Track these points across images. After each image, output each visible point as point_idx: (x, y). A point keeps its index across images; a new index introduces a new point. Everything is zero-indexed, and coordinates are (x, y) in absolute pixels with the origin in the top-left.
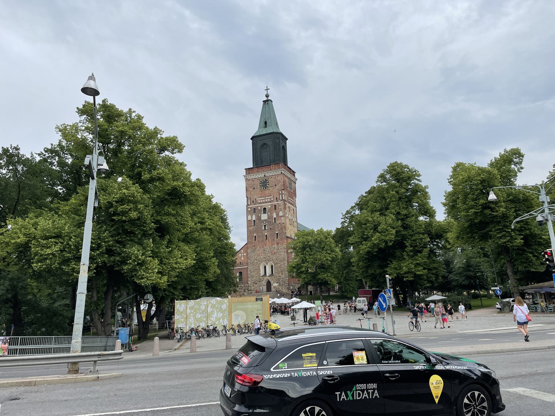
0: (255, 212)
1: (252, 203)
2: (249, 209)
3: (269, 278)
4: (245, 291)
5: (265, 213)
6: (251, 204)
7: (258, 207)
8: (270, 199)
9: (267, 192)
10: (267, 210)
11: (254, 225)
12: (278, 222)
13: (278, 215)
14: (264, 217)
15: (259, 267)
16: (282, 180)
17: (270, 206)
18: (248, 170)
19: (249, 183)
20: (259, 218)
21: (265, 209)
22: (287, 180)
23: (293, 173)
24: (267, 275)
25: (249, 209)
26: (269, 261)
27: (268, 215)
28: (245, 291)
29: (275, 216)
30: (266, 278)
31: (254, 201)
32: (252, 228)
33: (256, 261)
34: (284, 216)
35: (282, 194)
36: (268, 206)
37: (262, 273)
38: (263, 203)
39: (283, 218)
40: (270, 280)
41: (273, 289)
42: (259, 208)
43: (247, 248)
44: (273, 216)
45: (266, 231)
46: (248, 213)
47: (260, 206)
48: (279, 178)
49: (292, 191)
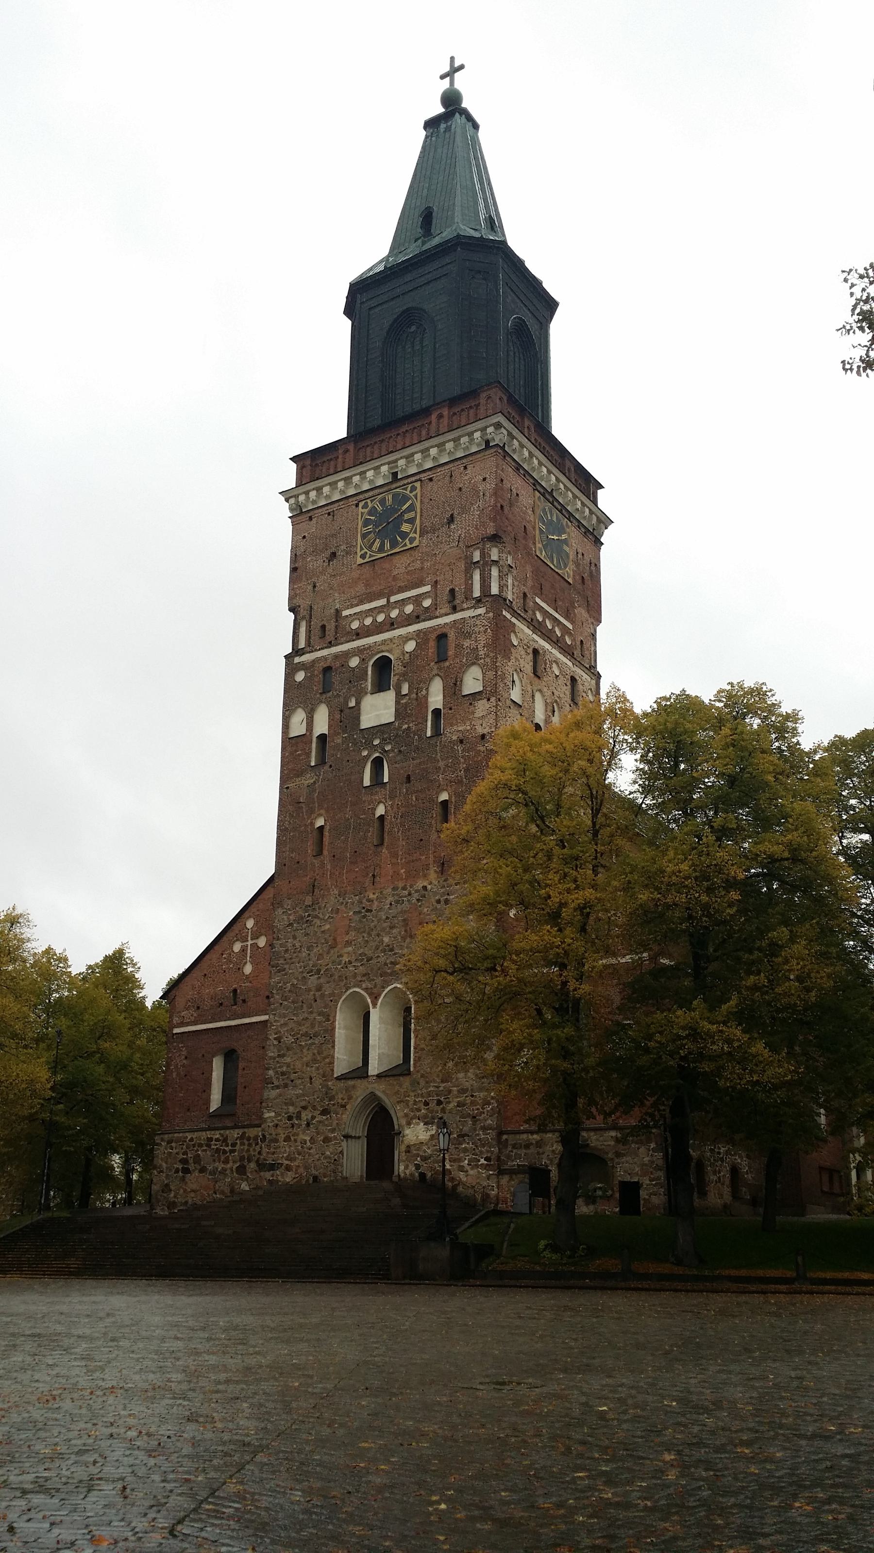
0: (326, 688)
1: (315, 639)
2: (300, 676)
3: (380, 1089)
4: (242, 1170)
5: (381, 686)
6: (310, 647)
7: (347, 655)
8: (417, 600)
9: (400, 565)
10: (397, 667)
11: (321, 761)
12: (452, 733)
13: (453, 689)
14: (378, 709)
15: (329, 1018)
16: (490, 486)
17: (410, 646)
18: (313, 464)
19: (312, 527)
20: (346, 719)
21: (383, 666)
22: (527, 498)
23: (589, 485)
24: (374, 1068)
25: (300, 676)
26: (388, 974)
27: (399, 696)
28: (242, 1170)
29: (436, 698)
30: (361, 1090)
31: (331, 627)
32: (308, 779)
33: (313, 981)
34: (492, 691)
35: (485, 564)
36: (402, 642)
37: (343, 1058)
38: (378, 628)
39: (482, 707)
40: (387, 1102)
41: (402, 1168)
42: (354, 662)
43: (277, 903)
44: (423, 702)
45: (381, 793)
46: (296, 696)
47: (358, 651)
48: (474, 474)
49: (569, 572)
